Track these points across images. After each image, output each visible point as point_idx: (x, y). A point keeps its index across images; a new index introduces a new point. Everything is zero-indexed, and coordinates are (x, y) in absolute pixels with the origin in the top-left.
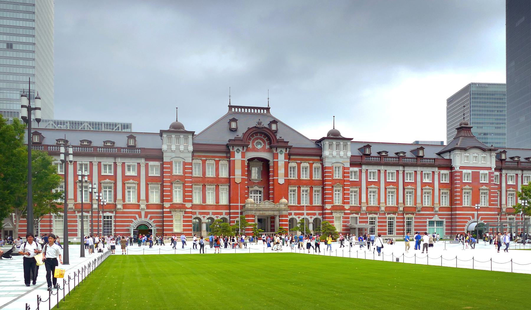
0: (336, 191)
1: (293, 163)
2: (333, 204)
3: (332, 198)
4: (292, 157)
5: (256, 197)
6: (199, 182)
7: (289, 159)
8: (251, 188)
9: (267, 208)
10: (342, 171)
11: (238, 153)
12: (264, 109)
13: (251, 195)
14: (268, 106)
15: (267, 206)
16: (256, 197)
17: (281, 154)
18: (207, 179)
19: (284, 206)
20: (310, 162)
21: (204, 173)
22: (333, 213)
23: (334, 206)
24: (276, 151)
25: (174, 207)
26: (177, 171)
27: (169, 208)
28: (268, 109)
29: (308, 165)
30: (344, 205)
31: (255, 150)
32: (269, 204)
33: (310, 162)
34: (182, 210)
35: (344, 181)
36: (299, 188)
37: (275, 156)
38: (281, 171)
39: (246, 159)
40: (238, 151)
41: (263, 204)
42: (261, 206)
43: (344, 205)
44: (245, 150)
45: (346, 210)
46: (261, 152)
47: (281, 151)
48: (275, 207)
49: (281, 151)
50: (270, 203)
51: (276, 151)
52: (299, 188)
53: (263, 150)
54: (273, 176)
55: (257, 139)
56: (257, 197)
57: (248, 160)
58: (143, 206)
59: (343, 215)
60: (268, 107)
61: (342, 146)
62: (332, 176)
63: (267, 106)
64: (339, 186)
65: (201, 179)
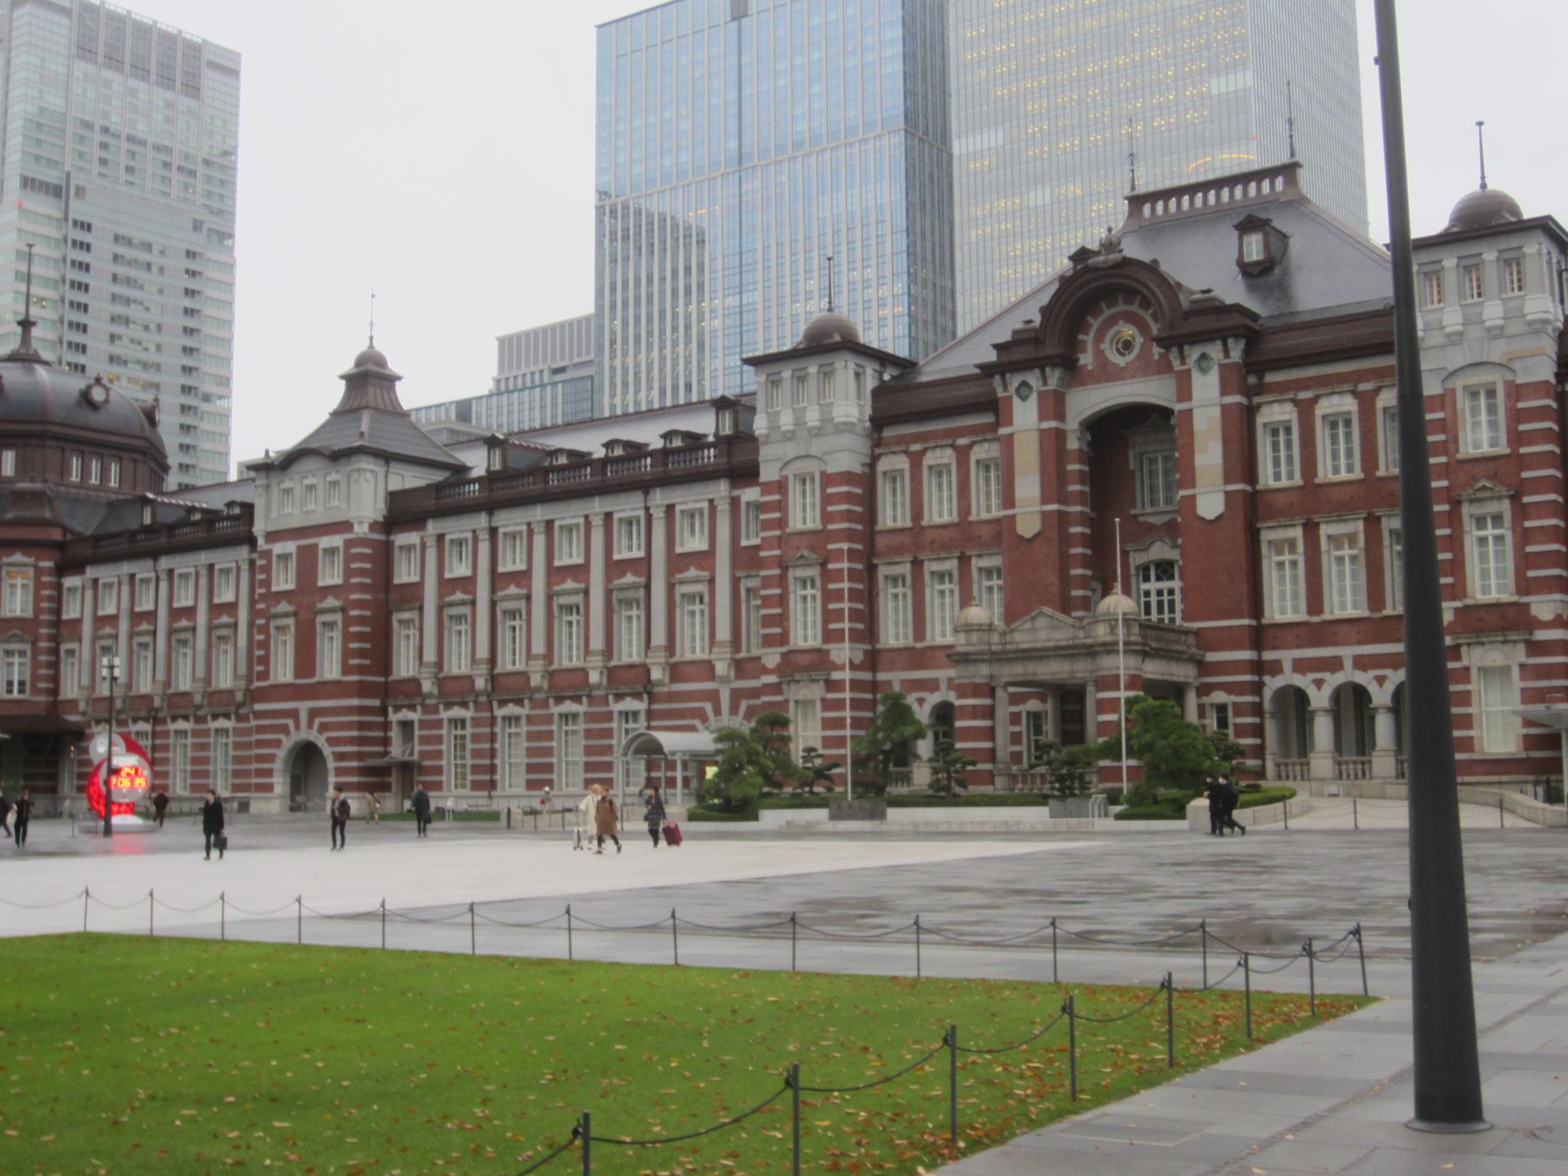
0: (1480, 522)
1: (1276, 407)
2: (1464, 595)
3: (1457, 566)
4: (1271, 378)
5: (1166, 593)
6: (899, 550)
7: (1248, 392)
8: (1137, 555)
9: (1044, 649)
10: (1507, 410)
11: (1024, 398)
12: (1270, 173)
13: (1144, 586)
14: (1292, 155)
15: (1043, 635)
16: (1166, 593)
17: (1204, 371)
18: (929, 535)
19: (1108, 631)
20: (1363, 387)
21: (965, 509)
22: (1464, 650)
23: (1467, 607)
24: (1183, 362)
25: (797, 666)
26: (804, 515)
27: (779, 670)
28: (1289, 170)
29: (1348, 404)
30: (1524, 599)
31: (1106, 373)
32: (1053, 627)
33: (1363, 387)
34: (815, 675)
35: (1522, 462)
36: (1311, 529)
37: (1184, 392)
38: (1209, 455)
39: (1072, 424)
40: (1024, 390)
41: (1027, 626)
42: (1018, 637)
43: (1524, 599)
44: (1053, 383)
45: (1534, 624)
46: (1132, 377)
47: (1204, 357)
48: (1077, 642)
49: (1204, 357)
50: (1056, 623)
51: (1183, 362)
52: (1311, 529)
53: (1146, 367)
54: (1183, 484)
55: (1112, 321)
56: (1171, 592)
57: (1081, 424)
58: (721, 668)
59: (1519, 655)
60: (1293, 160)
61: (1491, 273)
62: (1451, 447)
63: (1283, 158)
64: (1487, 494)
65: (906, 539)
